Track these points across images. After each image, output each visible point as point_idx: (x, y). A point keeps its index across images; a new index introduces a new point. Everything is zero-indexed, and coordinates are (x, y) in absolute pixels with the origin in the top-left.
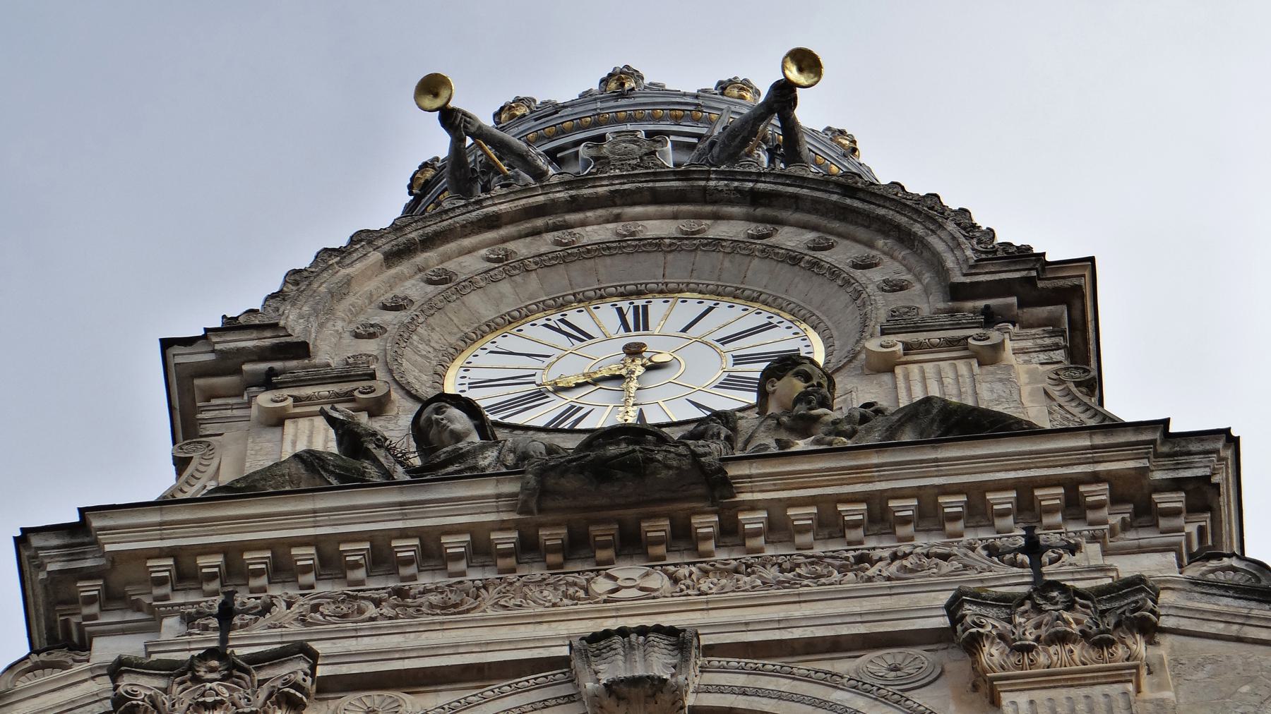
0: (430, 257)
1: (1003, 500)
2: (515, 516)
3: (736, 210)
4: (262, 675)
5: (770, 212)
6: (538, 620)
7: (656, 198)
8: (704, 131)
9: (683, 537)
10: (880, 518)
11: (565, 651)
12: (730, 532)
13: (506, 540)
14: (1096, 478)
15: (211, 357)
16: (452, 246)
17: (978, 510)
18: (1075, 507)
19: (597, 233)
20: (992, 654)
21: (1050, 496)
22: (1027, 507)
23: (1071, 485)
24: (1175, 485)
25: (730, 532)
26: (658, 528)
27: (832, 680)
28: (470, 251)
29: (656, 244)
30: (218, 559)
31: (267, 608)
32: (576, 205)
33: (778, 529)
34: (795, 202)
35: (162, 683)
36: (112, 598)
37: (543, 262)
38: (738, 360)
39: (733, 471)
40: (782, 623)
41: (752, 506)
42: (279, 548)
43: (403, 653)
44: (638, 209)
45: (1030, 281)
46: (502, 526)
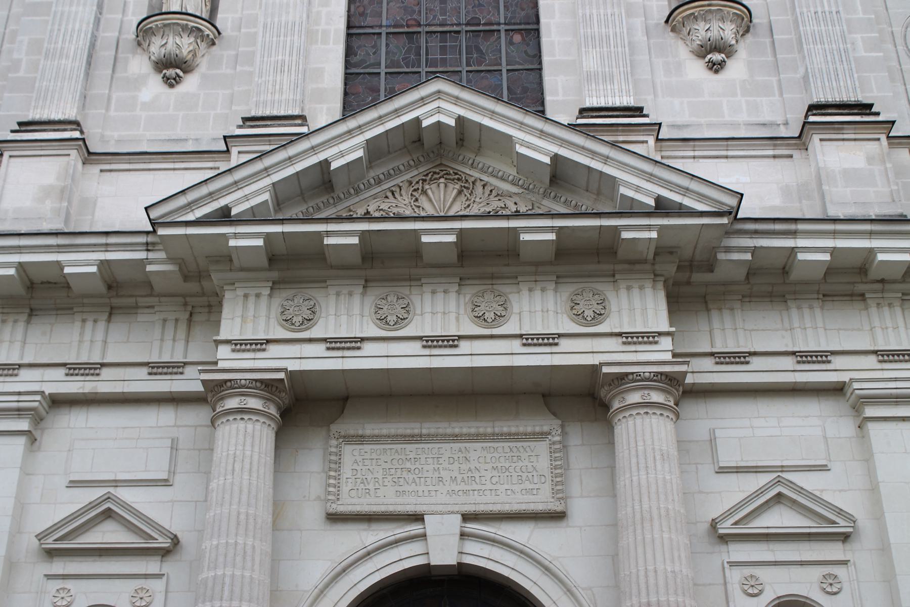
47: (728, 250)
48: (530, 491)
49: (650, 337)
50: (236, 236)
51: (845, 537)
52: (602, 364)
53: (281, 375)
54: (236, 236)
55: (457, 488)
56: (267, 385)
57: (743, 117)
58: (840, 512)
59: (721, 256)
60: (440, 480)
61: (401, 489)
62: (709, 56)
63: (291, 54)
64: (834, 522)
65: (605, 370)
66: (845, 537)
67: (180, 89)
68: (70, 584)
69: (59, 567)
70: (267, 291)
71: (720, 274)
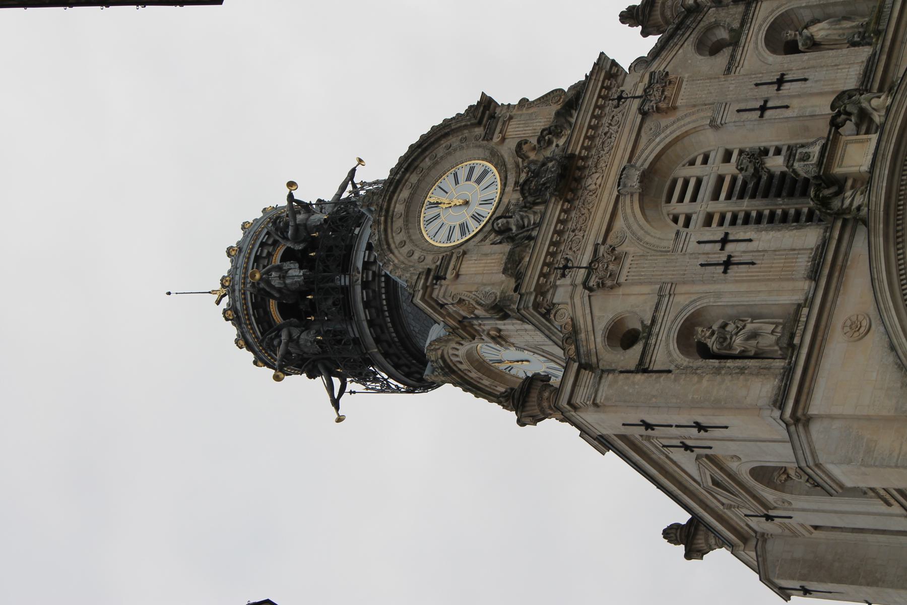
0: (393, 246)
1: (601, 102)
2: (561, 202)
3: (407, 175)
4: (601, 255)
5: (413, 167)
6: (600, 201)
7: (394, 192)
8: (265, 231)
9: (584, 168)
11: (616, 193)
13: (567, 205)
14: (603, 82)
15: (421, 292)
16: (391, 241)
18: (608, 88)
20: (663, 105)
22: (605, 98)
23: (602, 87)
26: (578, 173)
27: (650, 141)
28: (393, 238)
29: (412, 196)
30: (546, 268)
31: (567, 260)
32: (387, 211)
33: (588, 149)
34: (414, 160)
35: (594, 277)
36: (544, 294)
37: (407, 221)
38: (469, 178)
39: (569, 152)
40: (625, 150)
41: (580, 152)
42: (548, 253)
44: (395, 198)
45: (484, 107)
46: (563, 205)
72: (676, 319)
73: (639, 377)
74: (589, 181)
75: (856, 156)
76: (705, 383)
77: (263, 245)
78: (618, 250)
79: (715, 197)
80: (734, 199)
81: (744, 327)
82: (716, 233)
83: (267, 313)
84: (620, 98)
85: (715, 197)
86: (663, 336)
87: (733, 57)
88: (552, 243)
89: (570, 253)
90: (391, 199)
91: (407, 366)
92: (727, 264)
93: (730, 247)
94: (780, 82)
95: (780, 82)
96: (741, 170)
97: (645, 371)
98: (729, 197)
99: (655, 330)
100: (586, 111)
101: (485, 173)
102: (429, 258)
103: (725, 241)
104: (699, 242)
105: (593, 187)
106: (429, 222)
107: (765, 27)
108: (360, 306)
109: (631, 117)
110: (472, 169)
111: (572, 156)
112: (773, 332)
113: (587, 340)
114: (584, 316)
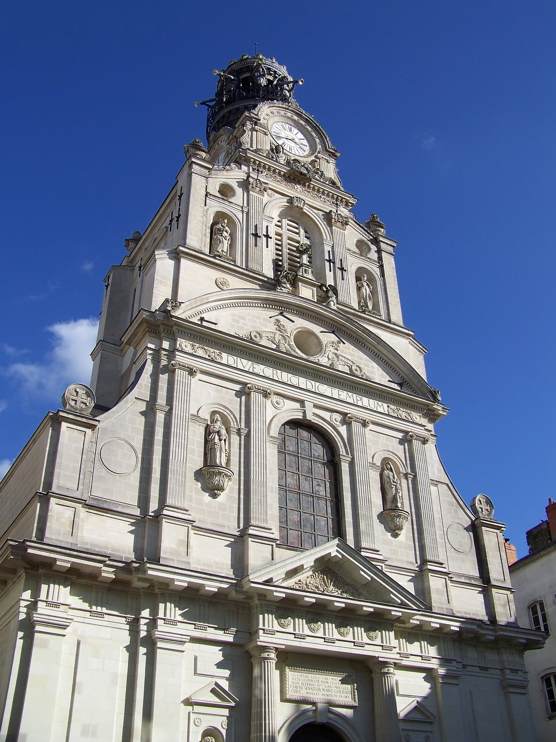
0: (271, 108)
1: (335, 197)
9: (304, 185)
10: (323, 193)
12: (309, 187)
13: (287, 175)
17: (333, 197)
19: (289, 115)
21: (340, 198)
23: (342, 198)
24: (351, 203)
25: (309, 187)
31: (262, 172)
32: (288, 109)
33: (314, 189)
36: (245, 160)
43: (276, 187)
47: (414, 619)
48: (346, 697)
49: (390, 649)
50: (276, 591)
51: (431, 723)
52: (378, 657)
53: (284, 647)
54: (276, 591)
55: (325, 693)
56: (277, 649)
57: (404, 558)
58: (432, 714)
59: (411, 621)
60: (319, 689)
61: (308, 691)
62: (397, 531)
63: (264, 497)
64: (430, 718)
65: (380, 659)
66: (431, 723)
67: (219, 499)
68: (200, 716)
69: (197, 708)
70: (274, 610)
71: (407, 625)
72: (231, 212)
73: (204, 193)
74: (298, 186)
75: (307, 292)
76: (200, 218)
77: (275, 72)
78: (265, 193)
79: (290, 239)
80: (288, 251)
81: (226, 239)
82: (272, 234)
83: (245, 72)
84: (337, 204)
85: (290, 239)
86: (223, 205)
87: (354, 252)
88: (270, 167)
89: (265, 174)
90: (293, 111)
91: (219, 126)
92: (256, 235)
93: (264, 239)
94: (342, 269)
95: (342, 269)
96: (302, 245)
97: (206, 195)
98: (289, 244)
99: (226, 203)
100: (331, 189)
101: (305, 151)
102: (265, 122)
103: (267, 236)
104: (267, 226)
105: (296, 187)
106: (283, 126)
107: (368, 268)
108: (246, 104)
109: (328, 207)
110: (306, 146)
111: (311, 180)
112: (222, 251)
113: (223, 175)
114: (235, 175)
